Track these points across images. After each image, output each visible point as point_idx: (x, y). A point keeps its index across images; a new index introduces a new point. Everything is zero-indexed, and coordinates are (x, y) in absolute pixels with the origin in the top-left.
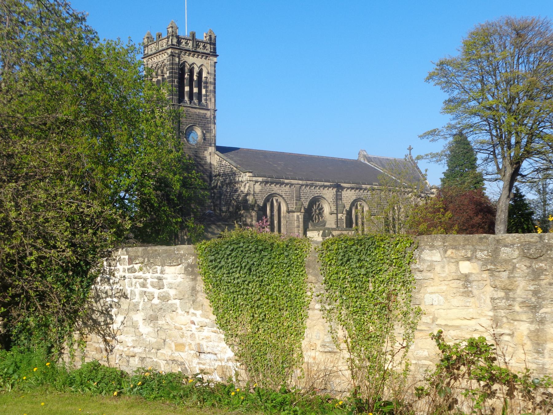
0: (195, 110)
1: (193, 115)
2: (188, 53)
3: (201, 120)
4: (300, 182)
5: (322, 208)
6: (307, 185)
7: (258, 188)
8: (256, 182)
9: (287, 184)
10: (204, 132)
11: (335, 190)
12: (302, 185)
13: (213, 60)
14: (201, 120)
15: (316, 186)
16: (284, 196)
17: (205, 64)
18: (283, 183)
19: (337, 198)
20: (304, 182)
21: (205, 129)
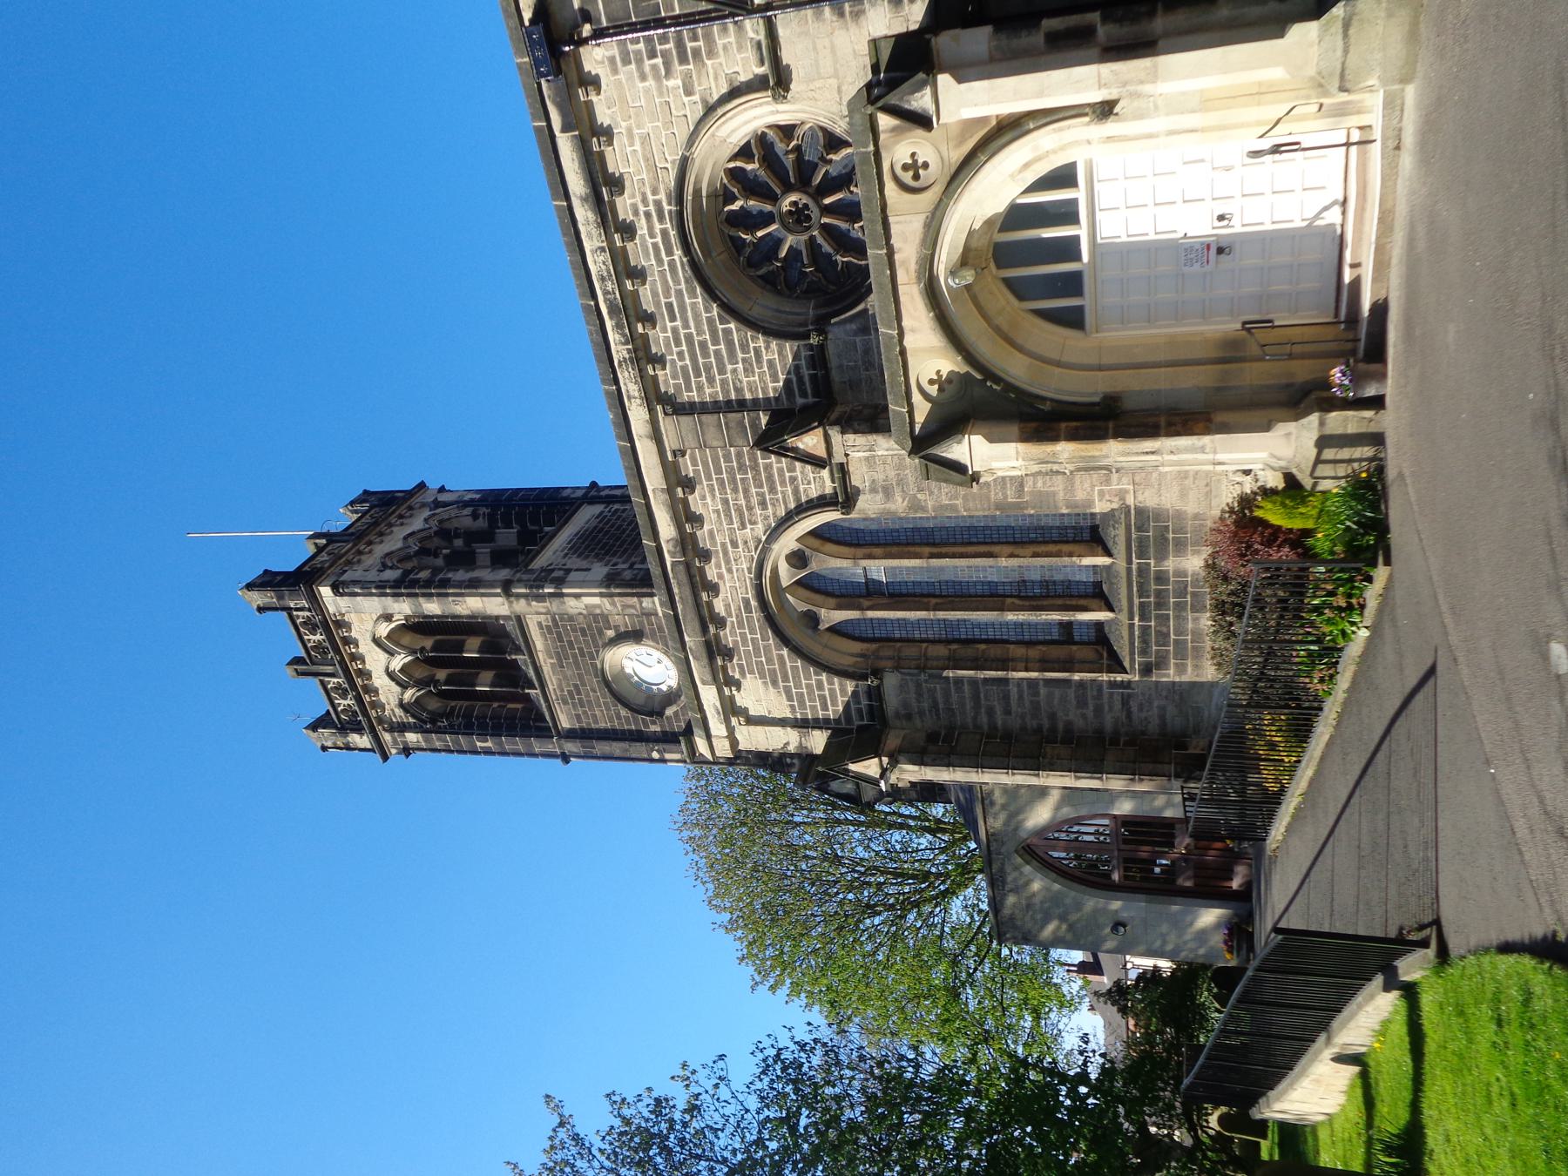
0: (547, 670)
1: (565, 677)
2: (367, 698)
3: (570, 643)
4: (638, 416)
5: (760, 147)
6: (643, 355)
7: (755, 695)
8: (730, 709)
9: (685, 517)
10: (610, 633)
11: (595, 57)
12: (655, 397)
13: (334, 601)
14: (572, 648)
15: (626, 271)
16: (760, 530)
17: (369, 626)
18: (687, 543)
19: (646, 26)
20: (630, 386)
21: (601, 633)
